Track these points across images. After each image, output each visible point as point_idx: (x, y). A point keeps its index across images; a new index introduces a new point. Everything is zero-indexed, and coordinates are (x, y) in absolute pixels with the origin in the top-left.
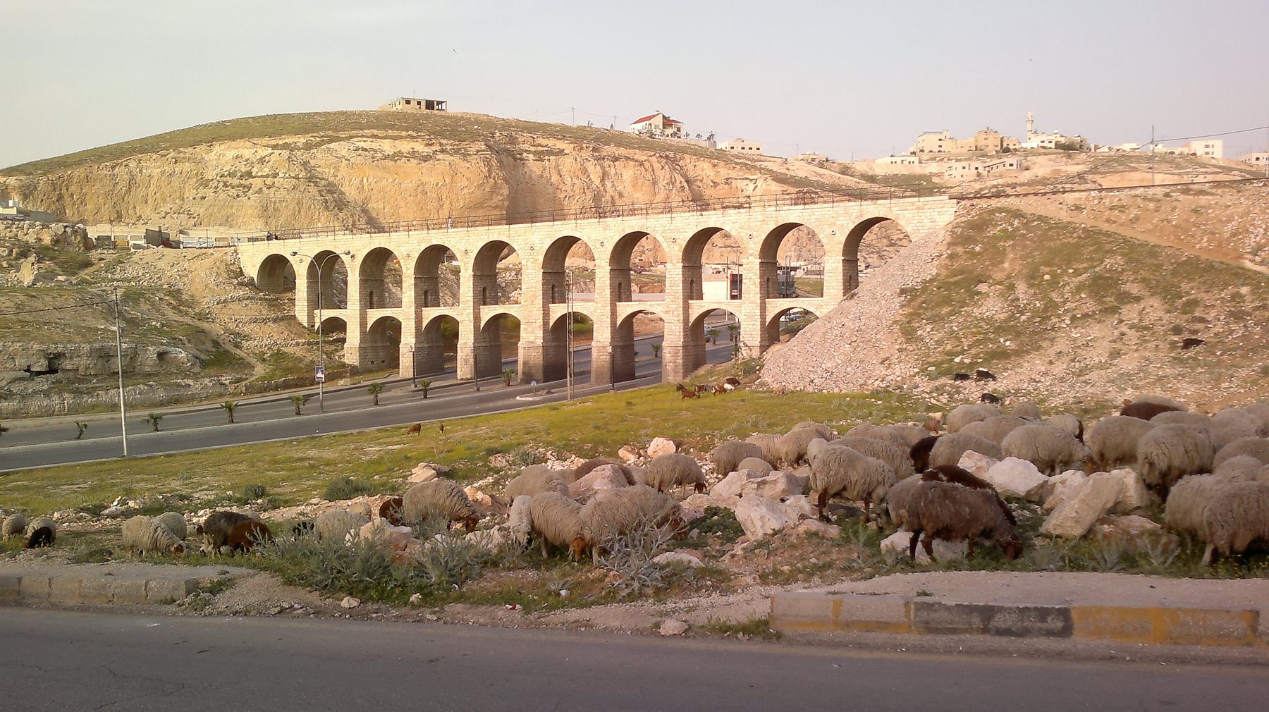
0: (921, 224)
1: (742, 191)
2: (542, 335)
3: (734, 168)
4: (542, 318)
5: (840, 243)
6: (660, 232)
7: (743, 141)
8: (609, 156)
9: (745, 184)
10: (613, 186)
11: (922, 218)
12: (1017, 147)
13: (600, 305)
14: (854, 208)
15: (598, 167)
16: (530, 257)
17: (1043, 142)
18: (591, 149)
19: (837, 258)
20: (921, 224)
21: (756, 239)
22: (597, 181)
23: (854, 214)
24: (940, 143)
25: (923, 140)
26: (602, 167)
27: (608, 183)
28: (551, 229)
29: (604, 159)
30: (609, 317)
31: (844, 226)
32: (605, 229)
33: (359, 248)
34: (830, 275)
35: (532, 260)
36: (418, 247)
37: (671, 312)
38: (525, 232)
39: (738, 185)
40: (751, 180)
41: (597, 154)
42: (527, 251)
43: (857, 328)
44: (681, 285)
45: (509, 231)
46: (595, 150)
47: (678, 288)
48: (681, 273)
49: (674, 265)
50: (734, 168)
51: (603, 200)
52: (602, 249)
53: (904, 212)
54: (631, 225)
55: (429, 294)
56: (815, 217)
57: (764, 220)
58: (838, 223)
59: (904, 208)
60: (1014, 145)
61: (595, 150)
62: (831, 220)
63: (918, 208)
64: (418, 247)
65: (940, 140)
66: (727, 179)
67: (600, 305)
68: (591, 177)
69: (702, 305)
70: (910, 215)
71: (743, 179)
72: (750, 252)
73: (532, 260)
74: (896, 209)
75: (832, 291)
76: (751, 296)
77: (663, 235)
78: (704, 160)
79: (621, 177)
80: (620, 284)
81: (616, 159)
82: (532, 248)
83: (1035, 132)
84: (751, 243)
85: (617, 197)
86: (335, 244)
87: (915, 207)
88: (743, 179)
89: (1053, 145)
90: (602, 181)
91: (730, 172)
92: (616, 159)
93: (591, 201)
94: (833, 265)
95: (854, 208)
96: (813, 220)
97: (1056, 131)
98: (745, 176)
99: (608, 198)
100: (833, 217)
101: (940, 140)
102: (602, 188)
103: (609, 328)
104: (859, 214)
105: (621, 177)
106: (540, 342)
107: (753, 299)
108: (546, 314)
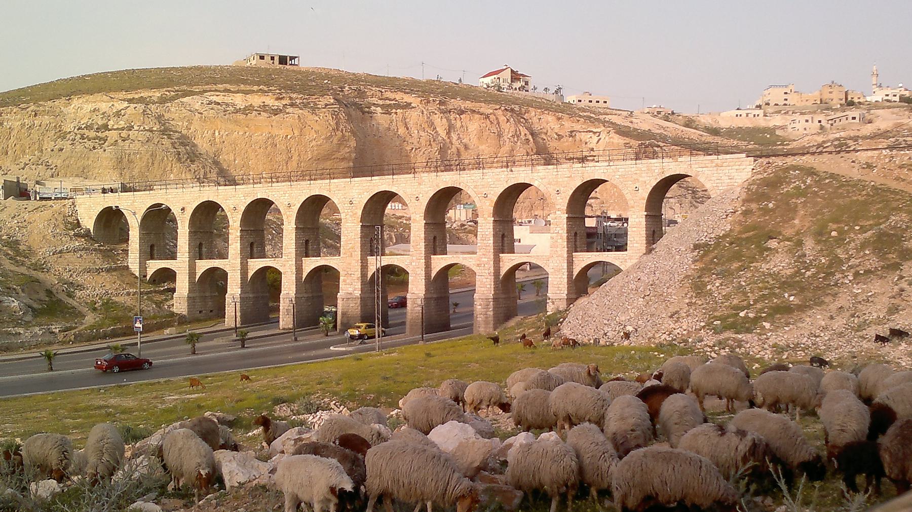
0: (720, 181)
1: (586, 143)
2: (360, 287)
3: (578, 121)
4: (360, 270)
5: (643, 199)
6: (472, 187)
7: (590, 95)
8: (455, 109)
9: (589, 136)
10: (459, 138)
11: (721, 175)
12: (861, 100)
13: (414, 258)
14: (656, 165)
15: (444, 120)
16: (349, 211)
17: (887, 95)
18: (438, 102)
19: (641, 213)
20: (720, 181)
21: (563, 194)
22: (443, 133)
23: (656, 171)
24: (786, 96)
25: (769, 94)
26: (449, 120)
27: (454, 136)
29: (450, 112)
30: (424, 269)
31: (648, 182)
32: (420, 184)
33: (189, 201)
34: (634, 229)
35: (351, 214)
36: (244, 201)
37: (482, 265)
38: (345, 187)
39: (582, 137)
40: (595, 133)
41: (443, 107)
42: (346, 205)
43: (651, 283)
44: (492, 239)
46: (441, 103)
47: (489, 242)
48: (492, 227)
49: (485, 219)
50: (578, 121)
51: (449, 151)
52: (417, 203)
53: (704, 169)
54: (445, 180)
55: (255, 246)
58: (641, 179)
59: (704, 166)
60: (859, 98)
61: (441, 103)
62: (635, 177)
63: (717, 165)
64: (244, 201)
65: (786, 93)
66: (571, 132)
67: (414, 258)
68: (438, 129)
69: (513, 258)
70: (710, 173)
71: (587, 132)
72: (558, 207)
73: (351, 214)
74: (697, 166)
76: (558, 249)
78: (548, 114)
79: (467, 130)
80: (435, 238)
81: (462, 112)
83: (880, 86)
85: (462, 149)
86: (166, 197)
87: (714, 164)
88: (587, 132)
89: (897, 99)
90: (448, 133)
91: (574, 125)
92: (462, 112)
93: (437, 153)
94: (637, 220)
95: (656, 165)
96: (618, 177)
97: (901, 85)
98: (589, 129)
99: (454, 150)
100: (636, 173)
101: (786, 93)
102: (448, 140)
103: (424, 280)
104: (660, 171)
105: (467, 130)
106: (358, 293)
107: (560, 253)
108: (364, 266)
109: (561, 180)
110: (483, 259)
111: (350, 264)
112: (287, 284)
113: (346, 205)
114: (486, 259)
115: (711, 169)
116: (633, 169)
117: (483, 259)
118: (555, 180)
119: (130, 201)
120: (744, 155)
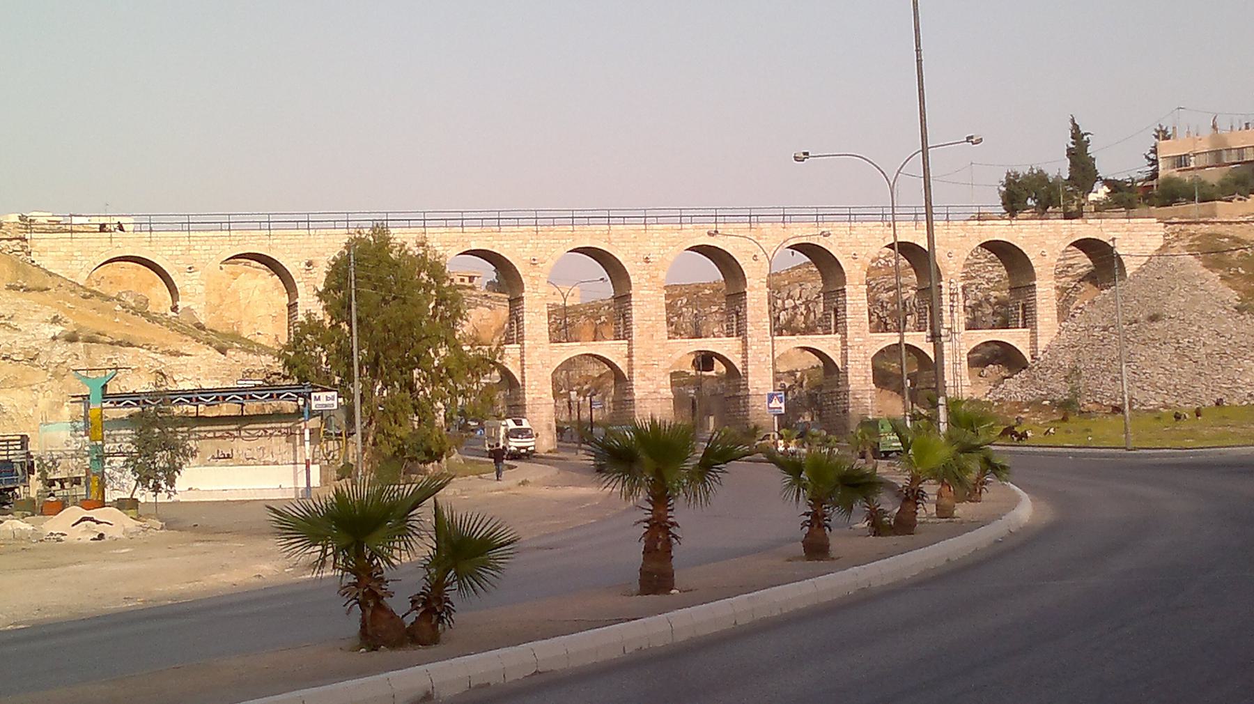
28: (676, 234)
31: (1056, 246)
33: (323, 251)
37: (856, 347)
38: (635, 237)
42: (639, 264)
45: (608, 234)
49: (856, 287)
52: (755, 264)
56: (1024, 235)
57: (965, 236)
58: (1047, 242)
62: (1041, 239)
69: (883, 339)
74: (1108, 230)
75: (1046, 320)
77: (841, 248)
82: (647, 260)
84: (951, 262)
87: (1125, 229)
100: (1042, 236)
104: (1070, 233)
109: (953, 240)
110: (856, 340)
111: (650, 350)
112: (536, 383)
113: (639, 264)
114: (861, 340)
115: (1123, 233)
116: (1039, 231)
117: (856, 340)
118: (946, 239)
119: (179, 248)
120: (1155, 220)
